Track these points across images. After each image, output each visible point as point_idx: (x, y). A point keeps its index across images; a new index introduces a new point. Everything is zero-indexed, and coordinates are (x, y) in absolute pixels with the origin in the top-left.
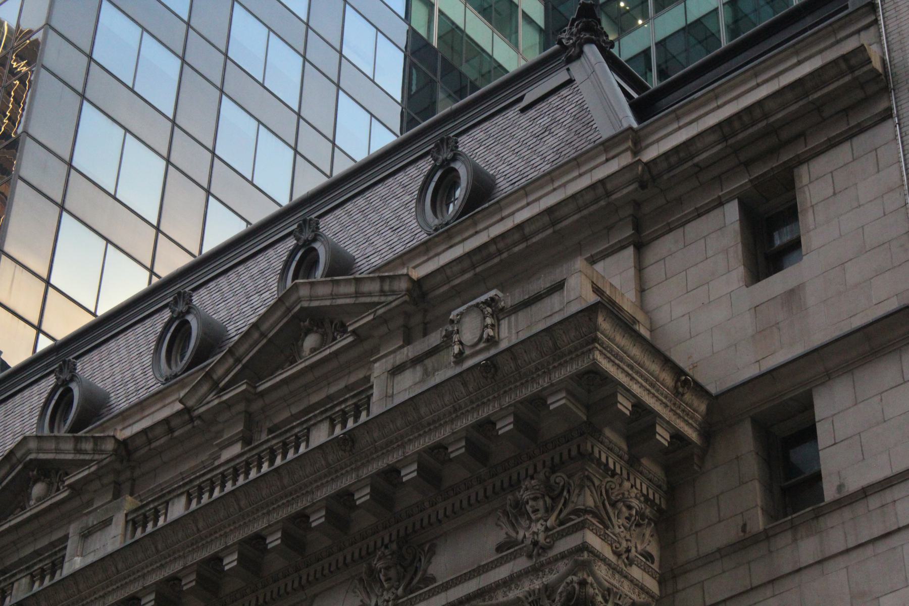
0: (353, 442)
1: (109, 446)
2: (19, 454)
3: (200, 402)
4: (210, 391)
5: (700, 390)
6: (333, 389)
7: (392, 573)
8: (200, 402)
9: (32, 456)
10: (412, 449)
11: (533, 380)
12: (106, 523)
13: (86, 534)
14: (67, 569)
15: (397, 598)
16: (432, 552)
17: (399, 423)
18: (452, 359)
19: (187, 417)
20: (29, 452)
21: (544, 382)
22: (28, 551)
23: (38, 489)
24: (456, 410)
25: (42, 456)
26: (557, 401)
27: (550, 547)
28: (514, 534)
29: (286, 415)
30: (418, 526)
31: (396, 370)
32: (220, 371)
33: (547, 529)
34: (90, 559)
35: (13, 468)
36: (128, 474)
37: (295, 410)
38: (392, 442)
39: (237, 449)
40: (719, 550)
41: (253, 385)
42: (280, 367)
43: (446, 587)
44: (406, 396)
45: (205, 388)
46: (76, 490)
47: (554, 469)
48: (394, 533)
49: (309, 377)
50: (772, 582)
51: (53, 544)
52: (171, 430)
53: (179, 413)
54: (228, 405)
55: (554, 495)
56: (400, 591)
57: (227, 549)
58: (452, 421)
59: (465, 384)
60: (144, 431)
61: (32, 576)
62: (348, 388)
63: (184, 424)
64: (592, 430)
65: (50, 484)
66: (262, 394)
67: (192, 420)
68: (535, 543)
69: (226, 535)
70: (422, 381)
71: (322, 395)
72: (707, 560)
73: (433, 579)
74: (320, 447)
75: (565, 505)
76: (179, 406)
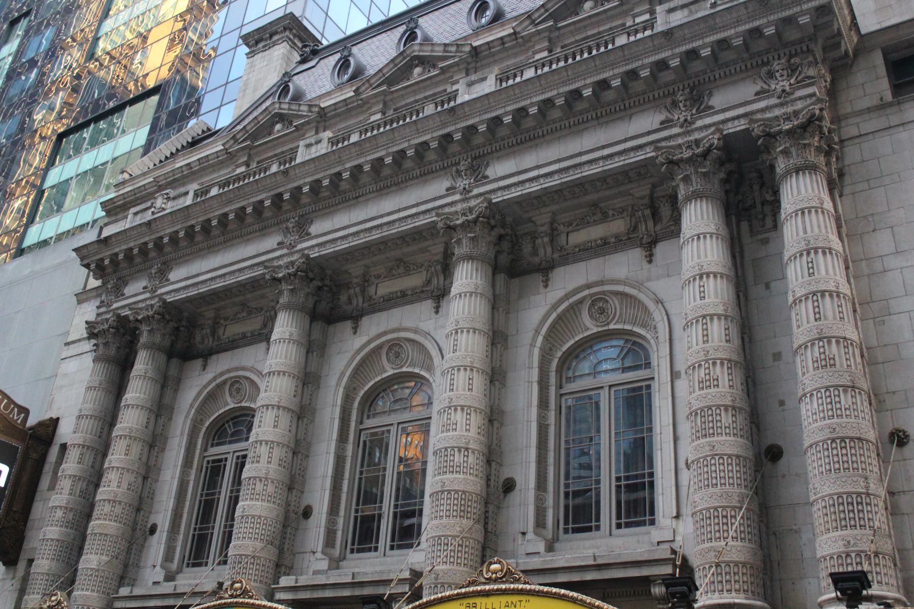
0: (672, 34)
1: (467, 49)
2: (408, 52)
3: (524, 29)
4: (530, 24)
5: (858, 30)
6: (601, 29)
7: (688, 103)
8: (524, 29)
9: (416, 54)
10: (708, 40)
11: (790, 8)
12: (484, 79)
13: (470, 84)
14: (459, 100)
15: (692, 115)
16: (710, 95)
17: (702, 26)
18: (709, 6)
19: (514, 37)
20: (414, 51)
21: (797, 9)
22: (412, 99)
23: (417, 70)
24: (738, 22)
25: (421, 54)
26: (804, 20)
27: (793, 94)
28: (765, 87)
29: (572, 40)
30: (702, 81)
31: (671, 11)
32: (536, 15)
33: (790, 84)
34: (474, 96)
35: (404, 59)
36: (473, 65)
37: (578, 38)
38: (695, 36)
39: (545, 54)
40: (868, 108)
41: (556, 22)
42: (570, 16)
43: (723, 111)
44: (679, 23)
45: (527, 22)
46: (444, 70)
47: (791, 56)
48: (686, 86)
49: (588, 22)
50: (903, 124)
51: (292, 149)
52: (503, 44)
53: (509, 35)
54: (539, 32)
55: (793, 70)
56: (694, 111)
57: (585, 86)
58: (735, 27)
59: (746, 8)
60: (488, 43)
61: (436, 104)
62: (611, 29)
63: (512, 41)
64: (813, 38)
65: (424, 68)
66: (559, 29)
67: (516, 39)
68: (784, 91)
69: (585, 79)
70: (689, 16)
71: (595, 31)
72: (860, 113)
73: (712, 108)
74: (622, 46)
75: (800, 74)
76: (512, 31)
